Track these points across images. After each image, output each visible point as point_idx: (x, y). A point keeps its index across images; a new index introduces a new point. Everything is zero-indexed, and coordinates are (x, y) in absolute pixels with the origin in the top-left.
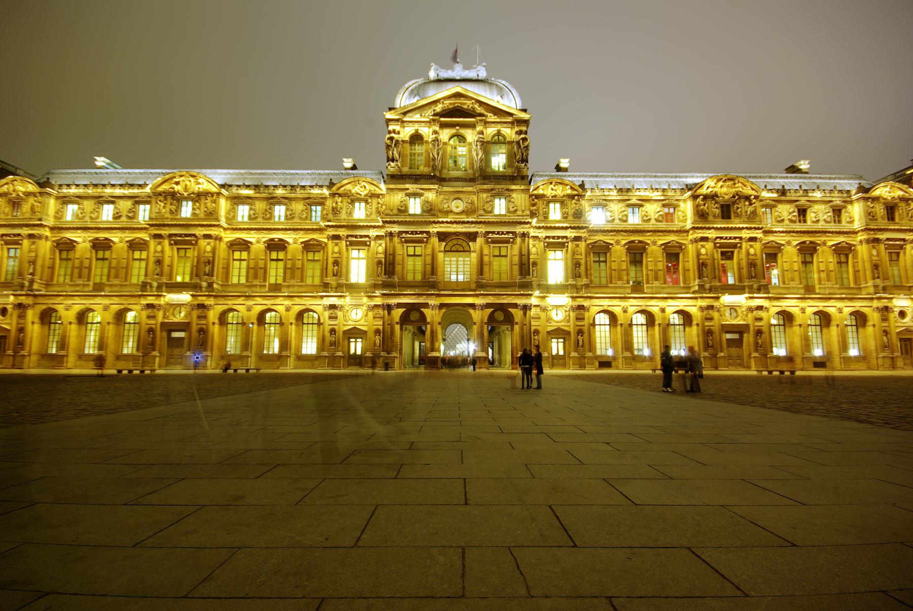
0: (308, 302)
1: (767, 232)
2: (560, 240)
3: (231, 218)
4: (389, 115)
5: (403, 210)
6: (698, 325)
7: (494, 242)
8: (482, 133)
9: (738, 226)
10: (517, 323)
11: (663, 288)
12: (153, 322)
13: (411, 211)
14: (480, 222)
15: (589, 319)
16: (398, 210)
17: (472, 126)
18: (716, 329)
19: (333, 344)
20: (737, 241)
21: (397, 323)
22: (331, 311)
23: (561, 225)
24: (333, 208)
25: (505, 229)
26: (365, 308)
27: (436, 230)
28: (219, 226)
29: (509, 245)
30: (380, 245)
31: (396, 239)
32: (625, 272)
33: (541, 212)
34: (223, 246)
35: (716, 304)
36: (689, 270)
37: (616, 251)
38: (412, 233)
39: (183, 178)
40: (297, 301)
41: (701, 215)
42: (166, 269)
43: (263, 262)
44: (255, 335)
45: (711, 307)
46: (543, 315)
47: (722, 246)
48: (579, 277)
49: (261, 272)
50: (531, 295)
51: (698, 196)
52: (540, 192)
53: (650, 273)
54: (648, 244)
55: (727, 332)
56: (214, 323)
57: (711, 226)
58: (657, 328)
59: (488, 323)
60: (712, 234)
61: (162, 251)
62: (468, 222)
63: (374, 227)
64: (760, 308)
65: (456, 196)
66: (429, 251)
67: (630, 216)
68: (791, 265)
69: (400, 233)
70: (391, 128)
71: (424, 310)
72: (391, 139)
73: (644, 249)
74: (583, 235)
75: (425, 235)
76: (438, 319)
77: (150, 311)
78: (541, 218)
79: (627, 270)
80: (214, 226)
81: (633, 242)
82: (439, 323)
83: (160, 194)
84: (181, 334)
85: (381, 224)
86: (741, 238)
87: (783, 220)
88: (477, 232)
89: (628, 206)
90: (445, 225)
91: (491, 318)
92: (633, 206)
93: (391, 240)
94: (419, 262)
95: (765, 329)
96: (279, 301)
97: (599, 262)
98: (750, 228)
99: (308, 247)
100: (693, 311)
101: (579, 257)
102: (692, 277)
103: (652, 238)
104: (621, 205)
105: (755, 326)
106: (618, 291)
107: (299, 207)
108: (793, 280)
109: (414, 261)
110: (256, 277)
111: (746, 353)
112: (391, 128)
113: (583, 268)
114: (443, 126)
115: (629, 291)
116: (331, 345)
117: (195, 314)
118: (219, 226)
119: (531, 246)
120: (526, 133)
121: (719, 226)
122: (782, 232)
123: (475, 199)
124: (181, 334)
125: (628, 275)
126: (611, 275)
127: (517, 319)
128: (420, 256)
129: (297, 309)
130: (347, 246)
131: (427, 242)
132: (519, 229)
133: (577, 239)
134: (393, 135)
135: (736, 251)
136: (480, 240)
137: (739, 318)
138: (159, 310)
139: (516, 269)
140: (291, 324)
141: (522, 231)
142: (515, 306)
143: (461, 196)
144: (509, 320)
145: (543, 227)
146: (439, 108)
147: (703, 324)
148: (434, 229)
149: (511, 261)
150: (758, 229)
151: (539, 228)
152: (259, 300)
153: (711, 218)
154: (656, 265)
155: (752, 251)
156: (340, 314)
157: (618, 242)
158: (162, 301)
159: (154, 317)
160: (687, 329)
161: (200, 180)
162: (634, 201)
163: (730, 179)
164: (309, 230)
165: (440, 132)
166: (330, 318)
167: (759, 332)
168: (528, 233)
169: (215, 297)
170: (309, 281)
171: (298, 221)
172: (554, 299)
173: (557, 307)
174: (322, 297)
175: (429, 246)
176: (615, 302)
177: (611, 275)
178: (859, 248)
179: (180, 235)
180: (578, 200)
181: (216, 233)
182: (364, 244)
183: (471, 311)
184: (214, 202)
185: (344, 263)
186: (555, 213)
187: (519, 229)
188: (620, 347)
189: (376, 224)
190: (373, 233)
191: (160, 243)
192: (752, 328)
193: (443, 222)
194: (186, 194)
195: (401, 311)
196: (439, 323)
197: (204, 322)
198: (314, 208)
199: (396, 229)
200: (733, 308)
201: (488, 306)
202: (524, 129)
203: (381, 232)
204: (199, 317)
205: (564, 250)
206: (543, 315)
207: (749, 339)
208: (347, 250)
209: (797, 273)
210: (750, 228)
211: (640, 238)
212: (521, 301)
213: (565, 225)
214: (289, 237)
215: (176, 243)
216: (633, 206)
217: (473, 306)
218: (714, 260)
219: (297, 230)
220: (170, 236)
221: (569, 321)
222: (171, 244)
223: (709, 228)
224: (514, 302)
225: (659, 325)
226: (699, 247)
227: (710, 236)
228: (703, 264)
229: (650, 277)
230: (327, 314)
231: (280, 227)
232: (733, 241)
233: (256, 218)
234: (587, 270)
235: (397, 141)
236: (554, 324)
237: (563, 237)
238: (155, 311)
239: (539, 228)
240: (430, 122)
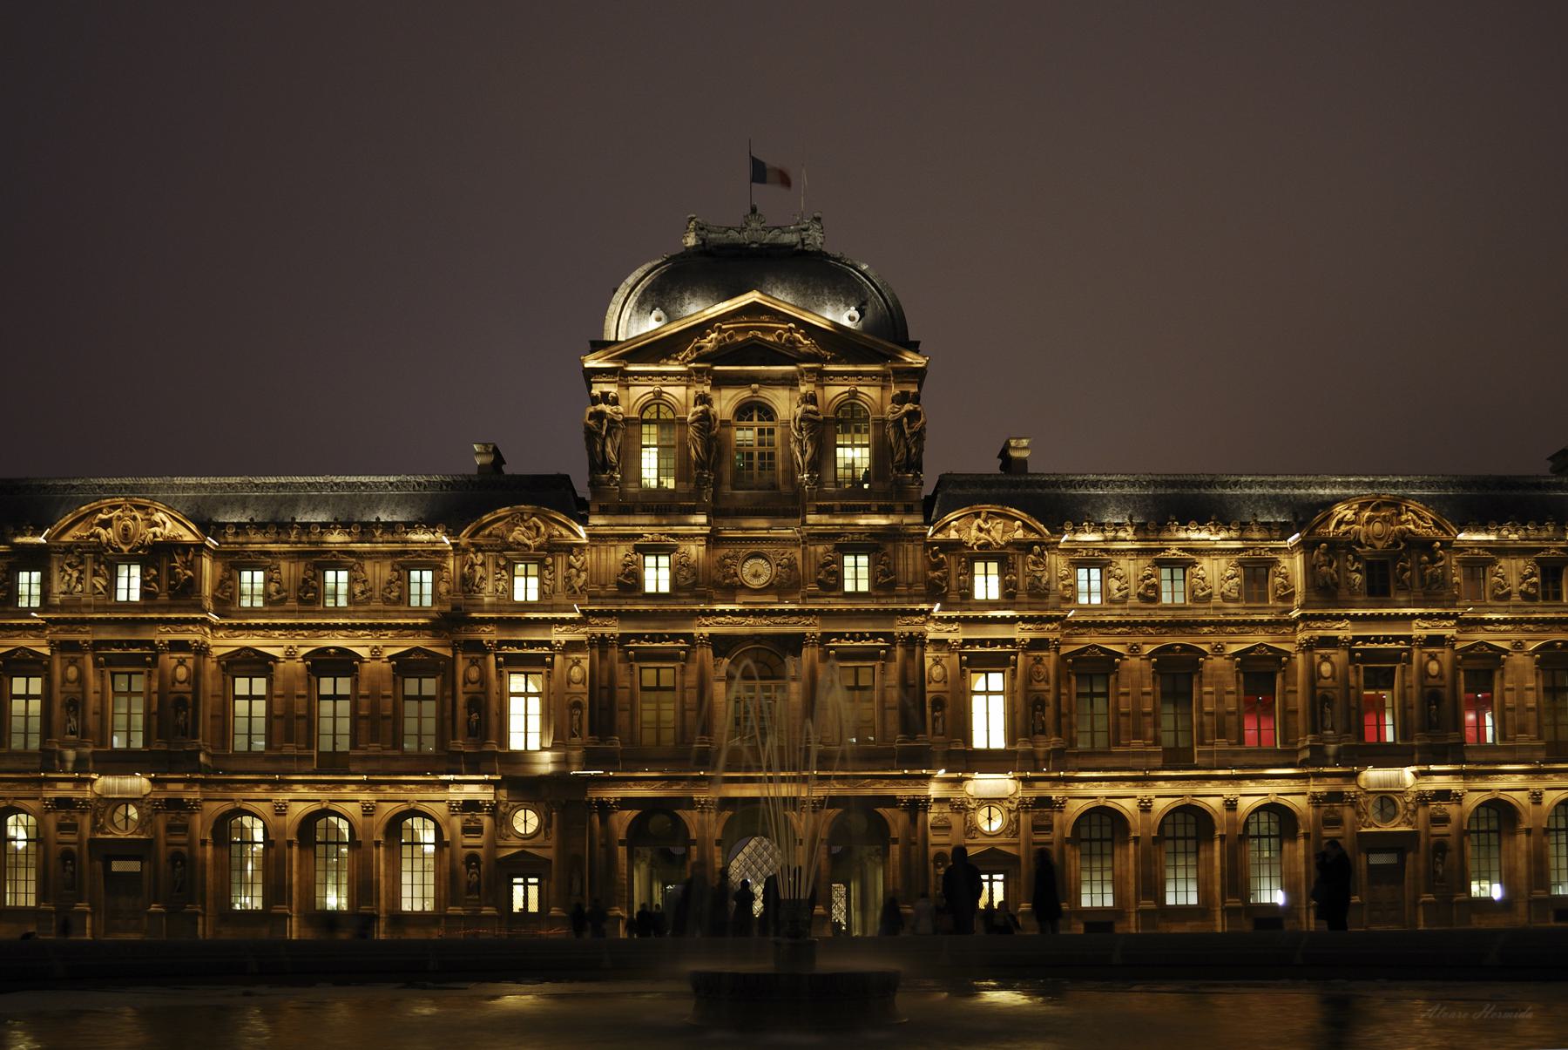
0: (416, 795)
1: (1466, 624)
2: (998, 649)
3: (227, 598)
4: (591, 363)
5: (631, 582)
6: (1307, 836)
7: (844, 655)
8: (811, 399)
9: (1402, 611)
10: (895, 841)
11: (1236, 754)
12: (73, 838)
13: (650, 588)
14: (811, 613)
15: (1062, 827)
16: (619, 583)
17: (790, 382)
18: (1346, 844)
19: (473, 888)
20: (1402, 645)
21: (622, 843)
22: (468, 816)
23: (999, 614)
24: (463, 576)
25: (867, 628)
27: (706, 631)
28: (204, 622)
29: (878, 664)
30: (577, 663)
31: (615, 653)
32: (1149, 719)
33: (953, 583)
34: (211, 666)
35: (1349, 789)
36: (1296, 712)
37: (1130, 670)
38: (652, 638)
39: (117, 512)
40: (390, 792)
41: (1324, 590)
42: (92, 721)
43: (303, 702)
44: (295, 868)
45: (1335, 797)
46: (956, 820)
47: (1368, 656)
48: (1043, 732)
50: (928, 778)
51: (1316, 545)
52: (953, 535)
53: (1205, 718)
54: (1204, 654)
55: (1370, 851)
56: (204, 843)
57: (1342, 612)
58: (1217, 843)
59: (831, 842)
61: (81, 679)
62: (781, 613)
63: (562, 622)
64: (1444, 795)
65: (754, 549)
66: (692, 679)
67: (1166, 586)
68: (1521, 696)
69: (625, 638)
70: (596, 391)
71: (685, 815)
72: (600, 416)
73: (1197, 666)
74: (1051, 636)
75: (682, 643)
76: (716, 831)
77: (63, 813)
78: (954, 597)
79: (1156, 715)
80: (194, 622)
81: (1169, 648)
82: (719, 843)
83: (69, 549)
84: (134, 866)
85: (576, 615)
86: (1408, 639)
87: (1509, 594)
89: (1161, 563)
91: (839, 832)
92: (1172, 564)
93: (603, 655)
94: (669, 711)
95: (1452, 842)
96: (347, 792)
97: (1092, 695)
98: (1429, 617)
100: (1299, 803)
101: (1043, 686)
102: (1301, 727)
103: (1214, 639)
104: (1144, 562)
105: (1429, 836)
106: (1132, 762)
107: (379, 573)
108: (1523, 730)
109: (658, 702)
110: (289, 737)
112: (596, 391)
113: (1050, 711)
114: (720, 382)
115: (1158, 761)
116: (470, 890)
117: (161, 821)
118: (204, 622)
119: (928, 662)
120: (916, 399)
121: (1360, 612)
122: (1505, 622)
123: (798, 555)
124: (134, 866)
125: (1156, 725)
126: (1117, 725)
127: (896, 832)
128: (673, 689)
129: (388, 809)
130: (498, 665)
131: (686, 659)
132: (901, 628)
133: (1037, 644)
134: (602, 407)
135: (1398, 667)
137: (1398, 819)
138: (83, 812)
139: (893, 718)
140: (377, 844)
141: (906, 630)
142: (891, 801)
143: (765, 549)
144: (879, 833)
145: (957, 619)
146: (710, 341)
147: (1318, 833)
148: (703, 629)
149: (883, 701)
150: (1447, 617)
151: (949, 620)
152: (303, 791)
153: (1343, 594)
154: (1220, 701)
155: (1433, 667)
157: (1134, 650)
158: (88, 793)
159: (73, 827)
160: (1286, 846)
161: (159, 517)
162: (1173, 551)
163: (1387, 504)
164: (407, 627)
165: (714, 395)
166: (465, 830)
167: (1440, 848)
168: (922, 635)
169: (203, 783)
170: (410, 745)
171: (381, 606)
172: (984, 784)
173: (990, 802)
174: (446, 784)
175: (693, 668)
176: (1122, 789)
177: (1117, 725)
179: (119, 644)
180: (1041, 555)
181: (198, 637)
182: (538, 661)
183: (793, 816)
184: (190, 565)
185: (494, 705)
186: (987, 584)
187: (901, 628)
188: (1132, 888)
189: (568, 616)
190: (559, 636)
191: (73, 662)
192: (1423, 840)
193: (723, 613)
195: (629, 815)
196: (719, 843)
197: (183, 840)
198: (415, 575)
199: (614, 629)
200: (1387, 799)
201: (832, 801)
202: (913, 389)
203: (579, 635)
204: (170, 828)
205: (1008, 670)
206: (956, 820)
207: (1415, 863)
208: (500, 675)
209: (1532, 715)
210: (1429, 617)
211: (1187, 641)
212: (903, 792)
213: (1008, 614)
214: (361, 646)
215: (111, 661)
216: (1172, 564)
218: (1348, 688)
219: (380, 627)
220: (98, 644)
221: (1016, 833)
222: (96, 664)
223: (1339, 618)
224: (889, 792)
225: (1222, 837)
226: (1317, 658)
227: (1341, 634)
228: (1325, 699)
229: (1208, 729)
230: (457, 822)
231: (341, 621)
232: (1392, 646)
233: (283, 601)
234: (1059, 715)
235: (612, 421)
236: (981, 840)
237: (1004, 642)
238: (75, 813)
239: (949, 620)
240: (687, 374)
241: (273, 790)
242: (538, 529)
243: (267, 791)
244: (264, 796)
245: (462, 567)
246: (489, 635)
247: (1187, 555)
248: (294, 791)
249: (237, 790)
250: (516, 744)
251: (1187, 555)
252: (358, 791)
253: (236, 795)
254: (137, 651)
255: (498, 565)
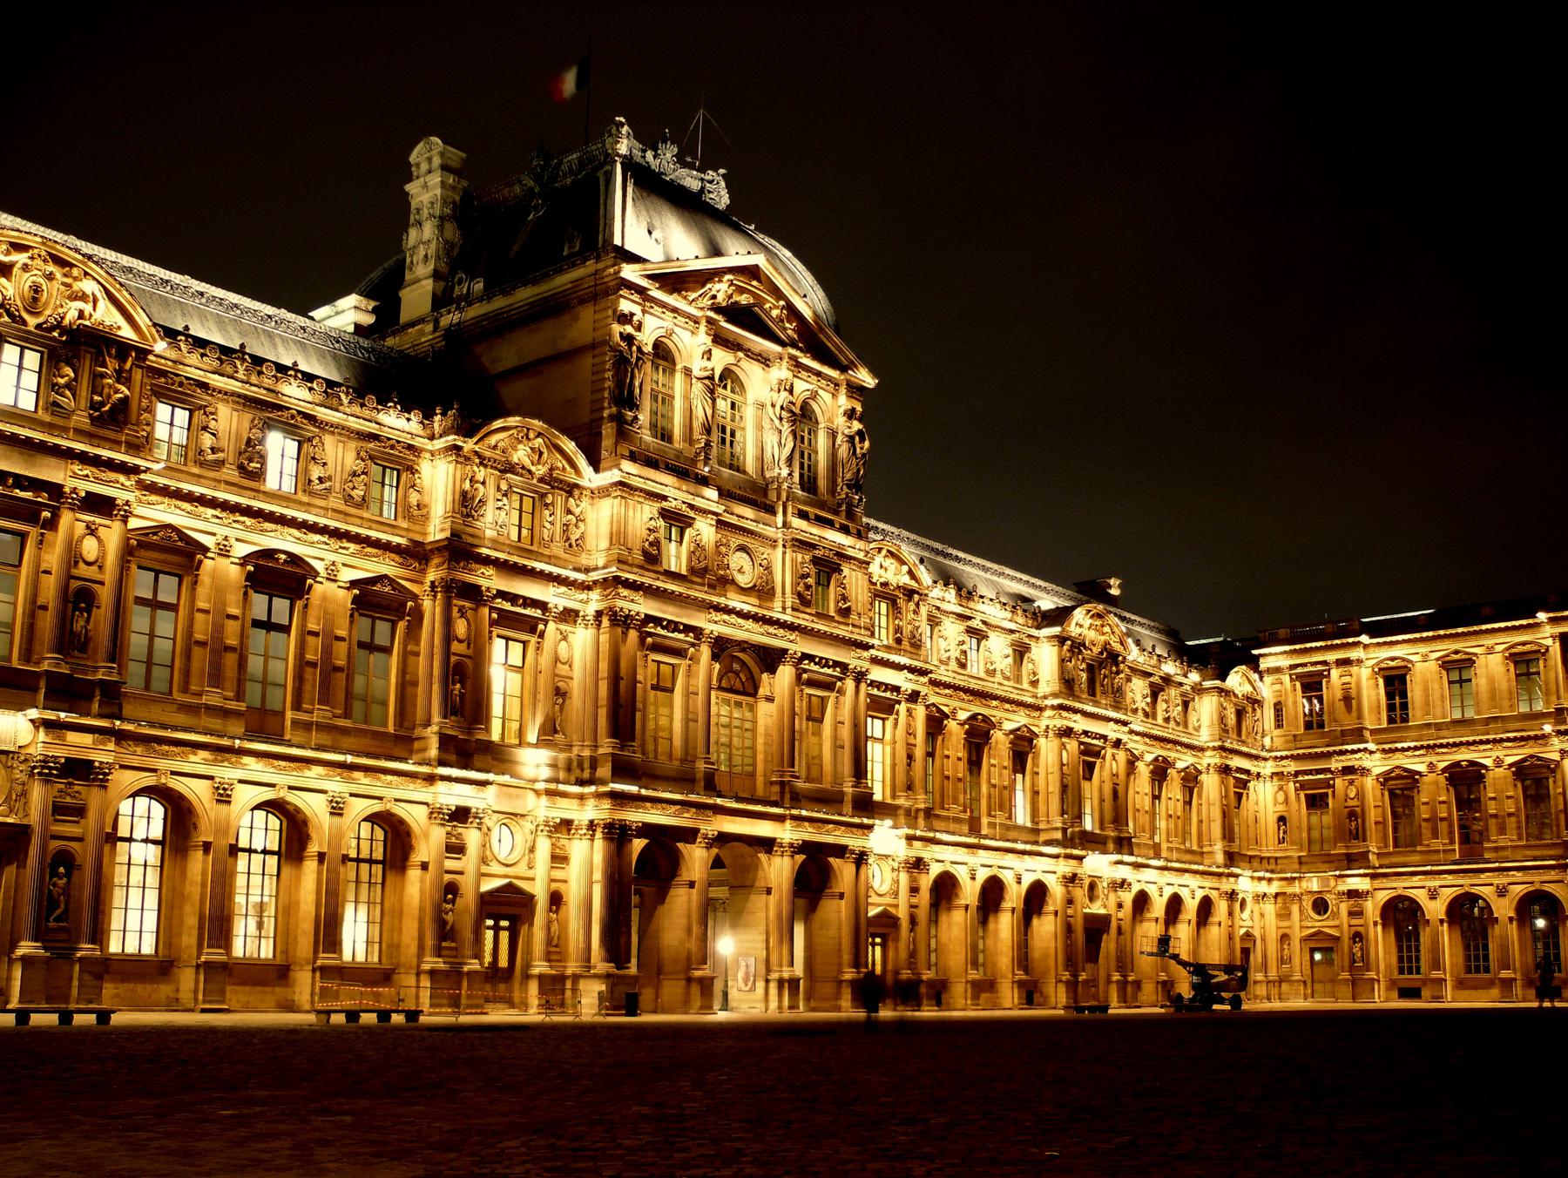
26: (528, 826)
40: (363, 782)
49: (231, 660)
60: (1079, 724)
72: (629, 339)
88: (785, 651)
90: (733, 619)
99: (371, 599)
111: (1102, 973)
114: (720, 340)
134: (629, 329)
136: (786, 672)
146: (721, 290)
156: (472, 837)
178: (1203, 777)
194: (32, 322)
217: (768, 844)
221: (896, 894)
241: (215, 762)
242: (541, 454)
243: (206, 762)
244: (202, 770)
245: (463, 480)
246: (490, 580)
247: (984, 628)
248: (244, 767)
249: (165, 755)
250: (495, 736)
251: (984, 628)
252: (327, 777)
253: (163, 764)
254: (28, 495)
255: (499, 489)
